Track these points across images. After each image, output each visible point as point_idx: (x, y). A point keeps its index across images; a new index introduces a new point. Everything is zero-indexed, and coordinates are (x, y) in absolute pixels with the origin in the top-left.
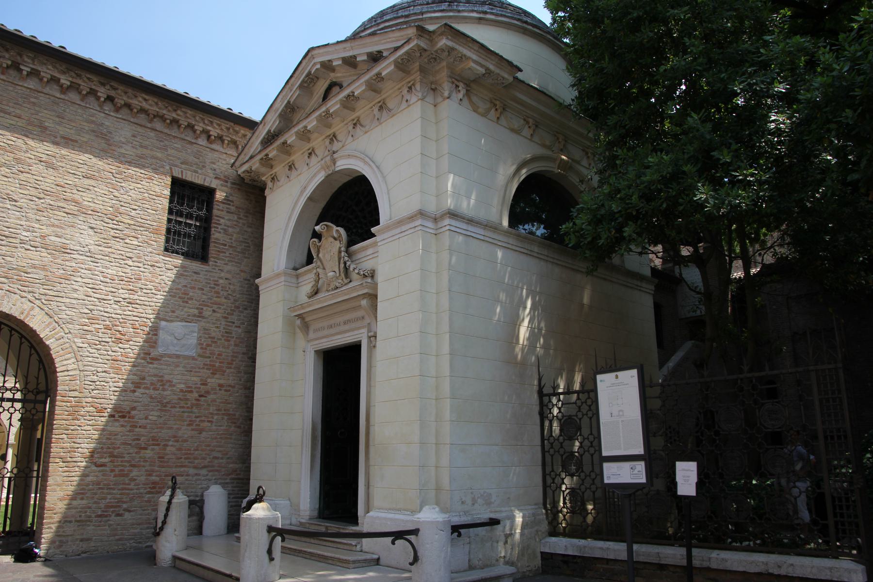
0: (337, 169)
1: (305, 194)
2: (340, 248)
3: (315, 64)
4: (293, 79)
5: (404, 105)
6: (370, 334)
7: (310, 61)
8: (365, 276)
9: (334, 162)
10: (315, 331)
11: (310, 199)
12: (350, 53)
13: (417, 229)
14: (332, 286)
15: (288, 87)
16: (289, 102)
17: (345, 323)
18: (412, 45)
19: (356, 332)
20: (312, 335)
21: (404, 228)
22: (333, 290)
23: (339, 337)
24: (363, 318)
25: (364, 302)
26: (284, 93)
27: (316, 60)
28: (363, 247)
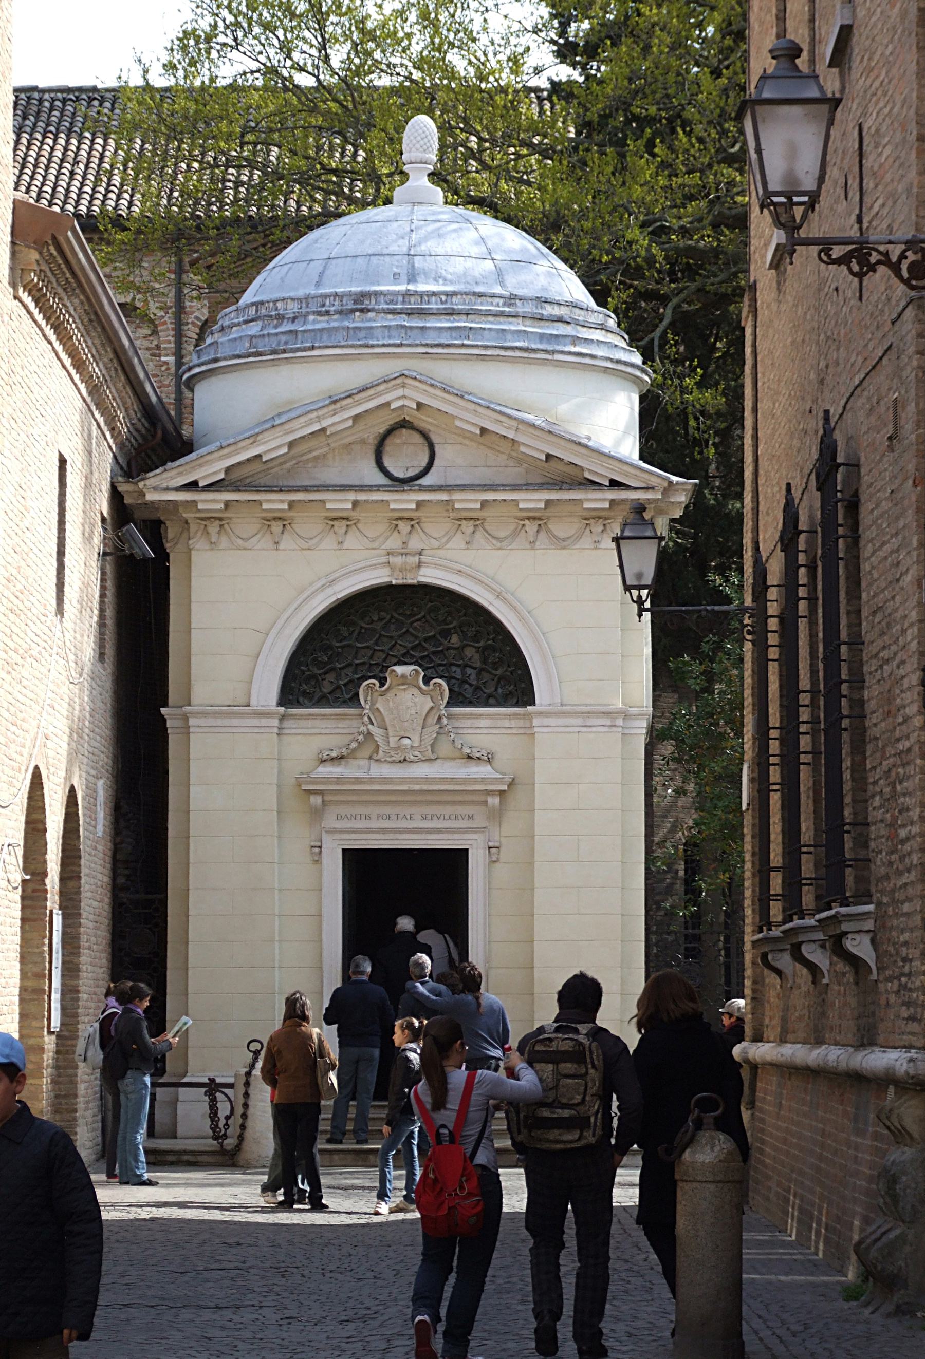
1: (329, 591)
2: (432, 708)
3: (404, 397)
4: (349, 400)
5: (586, 541)
6: (491, 844)
7: (396, 387)
10: (339, 818)
12: (511, 434)
13: (614, 729)
15: (333, 407)
16: (323, 430)
17: (425, 818)
18: (649, 495)
19: (456, 836)
20: (330, 821)
22: (393, 762)
25: (494, 801)
26: (320, 413)
27: (407, 392)
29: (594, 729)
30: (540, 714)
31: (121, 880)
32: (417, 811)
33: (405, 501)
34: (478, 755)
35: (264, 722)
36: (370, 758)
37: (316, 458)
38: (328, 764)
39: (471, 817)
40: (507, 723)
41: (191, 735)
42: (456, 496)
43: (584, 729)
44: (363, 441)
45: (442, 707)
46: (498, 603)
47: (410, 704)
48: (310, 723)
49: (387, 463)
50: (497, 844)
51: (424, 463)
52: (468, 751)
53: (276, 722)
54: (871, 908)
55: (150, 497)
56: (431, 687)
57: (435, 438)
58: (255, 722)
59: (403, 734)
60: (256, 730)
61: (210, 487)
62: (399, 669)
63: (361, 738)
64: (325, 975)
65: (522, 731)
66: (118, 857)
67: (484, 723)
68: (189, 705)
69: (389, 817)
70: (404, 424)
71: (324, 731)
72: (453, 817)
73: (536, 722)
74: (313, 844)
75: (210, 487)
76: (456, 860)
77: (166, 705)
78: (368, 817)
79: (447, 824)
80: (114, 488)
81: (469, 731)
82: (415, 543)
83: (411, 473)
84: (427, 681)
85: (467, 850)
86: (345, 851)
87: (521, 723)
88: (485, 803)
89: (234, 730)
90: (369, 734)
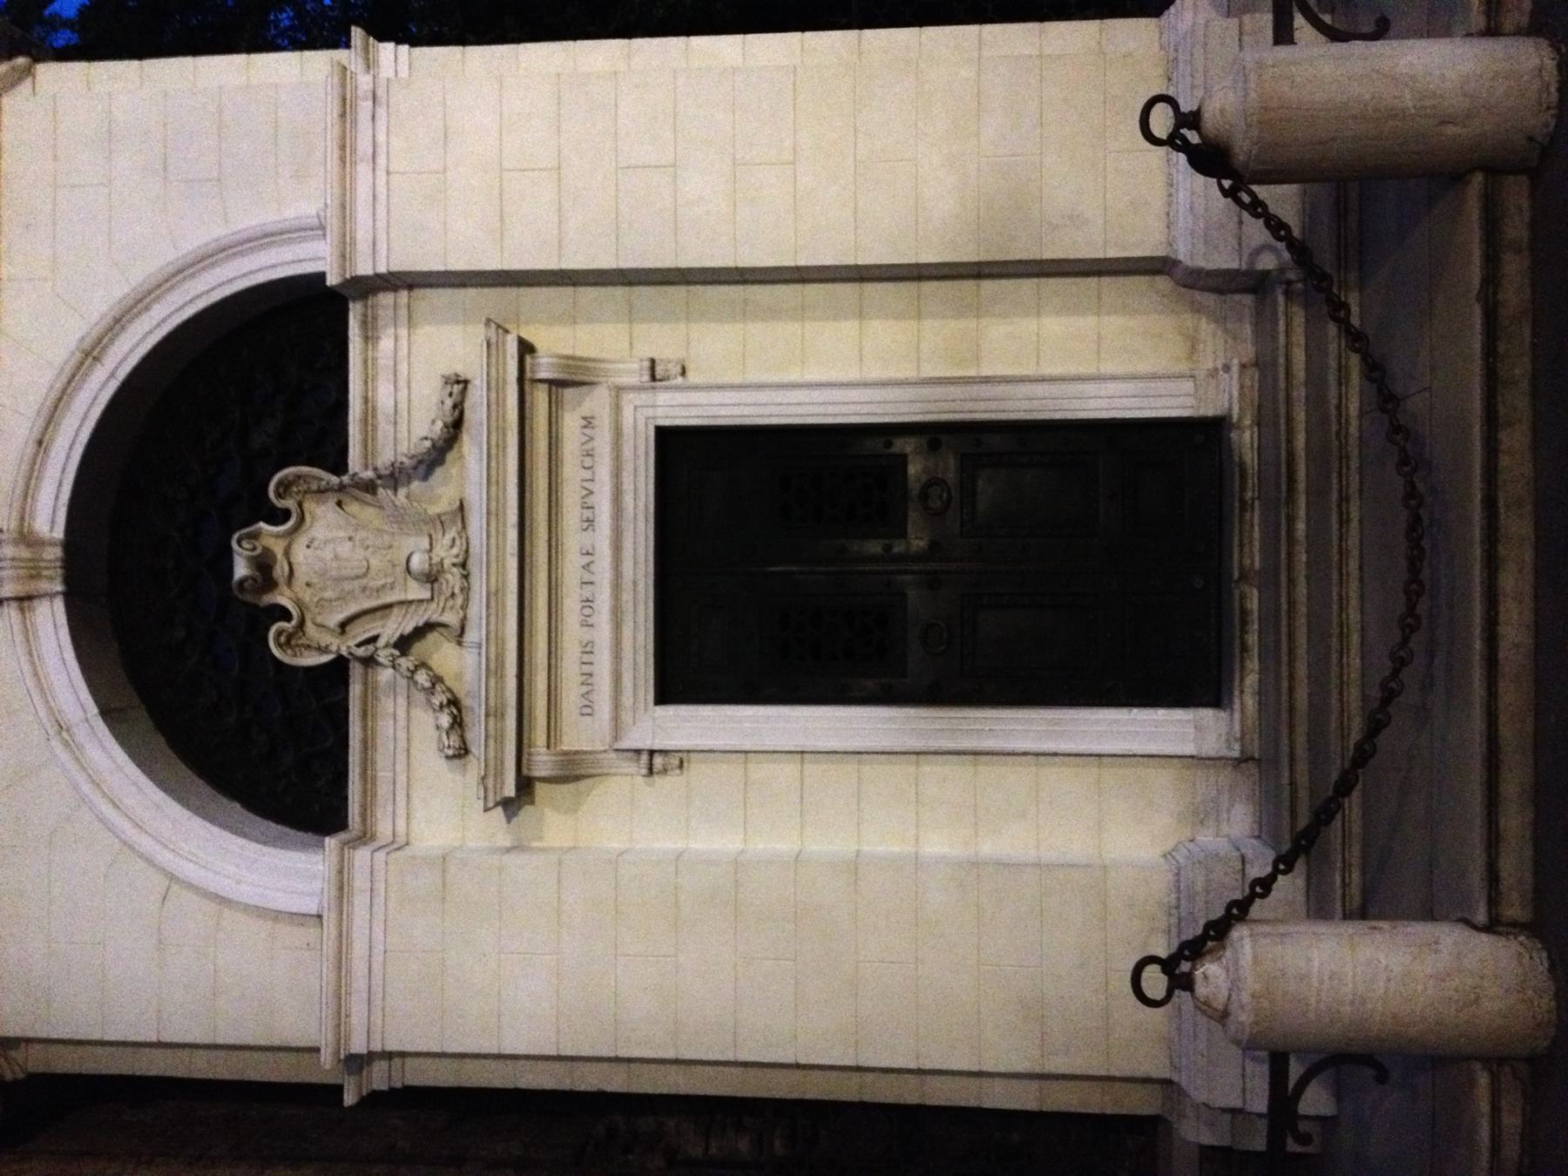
0: (59, 533)
1: (81, 733)
6: (646, 378)
8: (459, 407)
9: (26, 538)
10: (588, 710)
11: (106, 713)
13: (380, 92)
14: (453, 579)
17: (590, 523)
21: (364, 145)
22: (466, 590)
23: (628, 544)
24: (588, 422)
28: (365, 413)
29: (381, 138)
30: (344, 257)
32: (573, 539)
34: (449, 402)
35: (360, 881)
36: (460, 643)
38: (469, 736)
39: (588, 422)
40: (386, 344)
41: (392, 1046)
43: (382, 160)
45: (335, 480)
46: (110, 360)
47: (327, 554)
48: (383, 774)
50: (647, 364)
52: (440, 424)
53: (361, 856)
56: (289, 503)
58: (360, 903)
59: (400, 569)
60: (379, 900)
62: (241, 570)
63: (405, 663)
64: (935, 744)
65: (403, 312)
66: (697, 1152)
67: (384, 397)
68: (317, 1050)
69: (588, 602)
71: (402, 744)
72: (588, 462)
73: (364, 268)
74: (644, 771)
76: (678, 449)
77: (338, 1090)
78: (588, 649)
79: (604, 472)
81: (403, 427)
87: (384, 314)
88: (556, 384)
89: (379, 949)
90: (404, 644)
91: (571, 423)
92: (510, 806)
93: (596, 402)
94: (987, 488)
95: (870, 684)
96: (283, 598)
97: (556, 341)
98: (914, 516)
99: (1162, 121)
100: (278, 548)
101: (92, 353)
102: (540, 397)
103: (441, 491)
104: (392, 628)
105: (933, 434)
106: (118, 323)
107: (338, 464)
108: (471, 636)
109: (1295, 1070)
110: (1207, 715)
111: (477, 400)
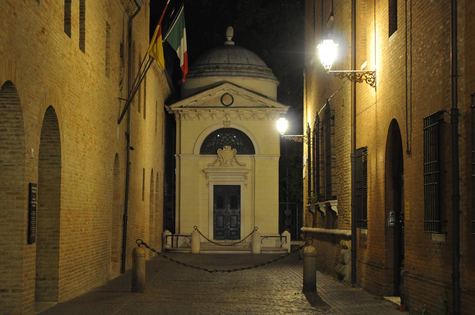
9: (229, 125)
10: (213, 178)
31: (165, 191)
32: (230, 177)
33: (227, 110)
37: (208, 101)
42: (239, 109)
44: (218, 97)
49: (223, 102)
51: (231, 102)
54: (337, 201)
55: (172, 109)
57: (233, 97)
61: (185, 107)
62: (226, 147)
70: (227, 94)
75: (185, 107)
78: (219, 178)
80: (165, 107)
82: (229, 119)
83: (229, 104)
84: (232, 149)
85: (240, 186)
86: (214, 186)
91: (241, 177)
92: (203, 171)
93: (243, 179)
94: (235, 218)
95: (215, 206)
96: (224, 149)
97: (249, 175)
98: (232, 210)
99: (256, 228)
100: (229, 149)
101: (248, 131)
102: (243, 174)
103: (234, 164)
104: (221, 160)
105: (240, 212)
106: (251, 133)
107: (237, 154)
108: (220, 167)
109: (190, 237)
110: (213, 238)
111: (244, 167)
